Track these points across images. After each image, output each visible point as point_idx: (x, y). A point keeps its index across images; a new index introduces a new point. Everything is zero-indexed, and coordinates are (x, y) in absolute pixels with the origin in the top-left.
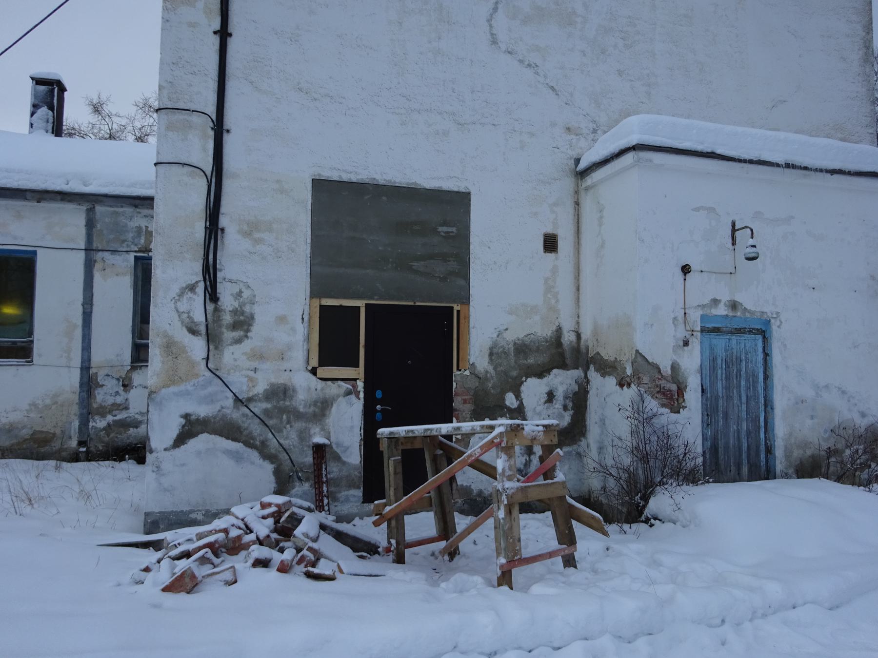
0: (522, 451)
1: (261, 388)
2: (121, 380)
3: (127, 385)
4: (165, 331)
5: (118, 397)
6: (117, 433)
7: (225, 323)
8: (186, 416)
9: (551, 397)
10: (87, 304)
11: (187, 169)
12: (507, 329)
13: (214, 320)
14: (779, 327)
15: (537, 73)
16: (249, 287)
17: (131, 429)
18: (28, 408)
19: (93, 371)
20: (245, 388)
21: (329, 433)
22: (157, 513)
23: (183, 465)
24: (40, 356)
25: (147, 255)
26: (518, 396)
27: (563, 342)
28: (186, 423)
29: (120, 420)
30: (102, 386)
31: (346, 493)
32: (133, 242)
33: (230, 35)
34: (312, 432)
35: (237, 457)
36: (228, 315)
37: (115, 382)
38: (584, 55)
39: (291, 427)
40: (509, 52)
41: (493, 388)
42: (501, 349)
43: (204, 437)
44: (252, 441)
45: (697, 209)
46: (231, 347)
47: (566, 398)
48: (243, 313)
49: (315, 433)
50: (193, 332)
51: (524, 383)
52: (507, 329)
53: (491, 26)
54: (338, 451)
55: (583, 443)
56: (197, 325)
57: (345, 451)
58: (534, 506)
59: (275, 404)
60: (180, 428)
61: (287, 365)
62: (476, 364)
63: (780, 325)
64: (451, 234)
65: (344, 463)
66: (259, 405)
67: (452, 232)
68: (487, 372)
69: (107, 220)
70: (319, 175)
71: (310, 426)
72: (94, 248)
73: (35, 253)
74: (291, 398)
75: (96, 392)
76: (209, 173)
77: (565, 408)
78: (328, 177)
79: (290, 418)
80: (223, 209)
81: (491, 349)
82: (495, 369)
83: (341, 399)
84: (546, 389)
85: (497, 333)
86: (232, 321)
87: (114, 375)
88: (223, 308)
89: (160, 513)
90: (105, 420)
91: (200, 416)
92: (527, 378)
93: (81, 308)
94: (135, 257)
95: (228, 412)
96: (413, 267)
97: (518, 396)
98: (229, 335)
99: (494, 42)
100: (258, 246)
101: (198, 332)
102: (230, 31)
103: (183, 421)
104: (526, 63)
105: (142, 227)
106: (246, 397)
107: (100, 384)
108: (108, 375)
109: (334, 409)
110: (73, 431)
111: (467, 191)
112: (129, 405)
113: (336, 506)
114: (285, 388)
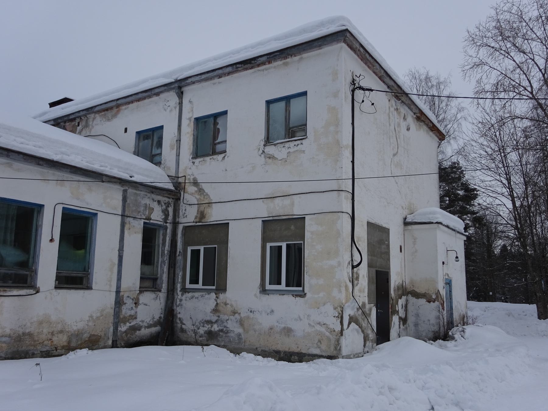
3: (136, 304)
6: (131, 335)
10: (121, 250)
11: (348, 215)
17: (137, 331)
18: (88, 319)
19: (121, 294)
24: (96, 283)
29: (133, 326)
30: (126, 303)
33: (351, 162)
35: (358, 332)
37: (131, 301)
50: (350, 281)
69: (132, 198)
70: (368, 220)
72: (126, 215)
73: (96, 214)
75: (123, 307)
83: (373, 308)
89: (346, 355)
90: (125, 326)
93: (118, 252)
94: (144, 222)
108: (128, 297)
110: (110, 334)
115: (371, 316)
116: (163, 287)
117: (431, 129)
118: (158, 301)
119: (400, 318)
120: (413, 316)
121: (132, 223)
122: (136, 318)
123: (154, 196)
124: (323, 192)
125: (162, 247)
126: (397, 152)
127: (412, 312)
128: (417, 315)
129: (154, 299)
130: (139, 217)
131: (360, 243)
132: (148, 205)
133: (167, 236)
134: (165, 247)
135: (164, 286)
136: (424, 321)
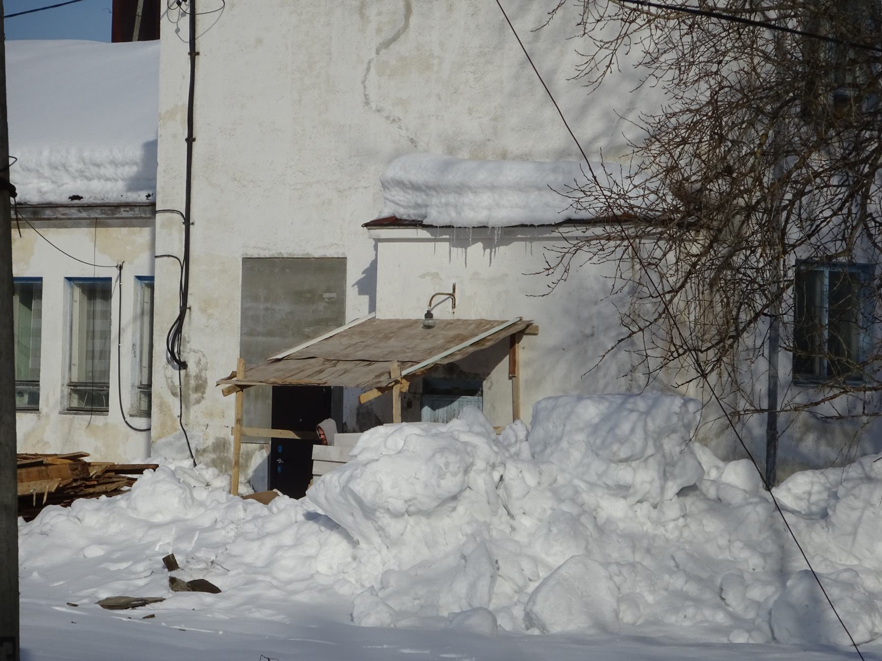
1: (210, 442)
14: (490, 388)
15: (400, 128)
20: (201, 440)
38: (440, 99)
40: (379, 111)
42: (365, 410)
45: (423, 276)
50: (174, 394)
53: (365, 87)
62: (347, 424)
63: (491, 386)
64: (332, 300)
67: (333, 298)
70: (246, 254)
78: (252, 255)
80: (190, 291)
81: (358, 409)
98: (194, 396)
99: (367, 103)
104: (391, 119)
106: (202, 448)
111: (344, 256)
131: (210, 311)
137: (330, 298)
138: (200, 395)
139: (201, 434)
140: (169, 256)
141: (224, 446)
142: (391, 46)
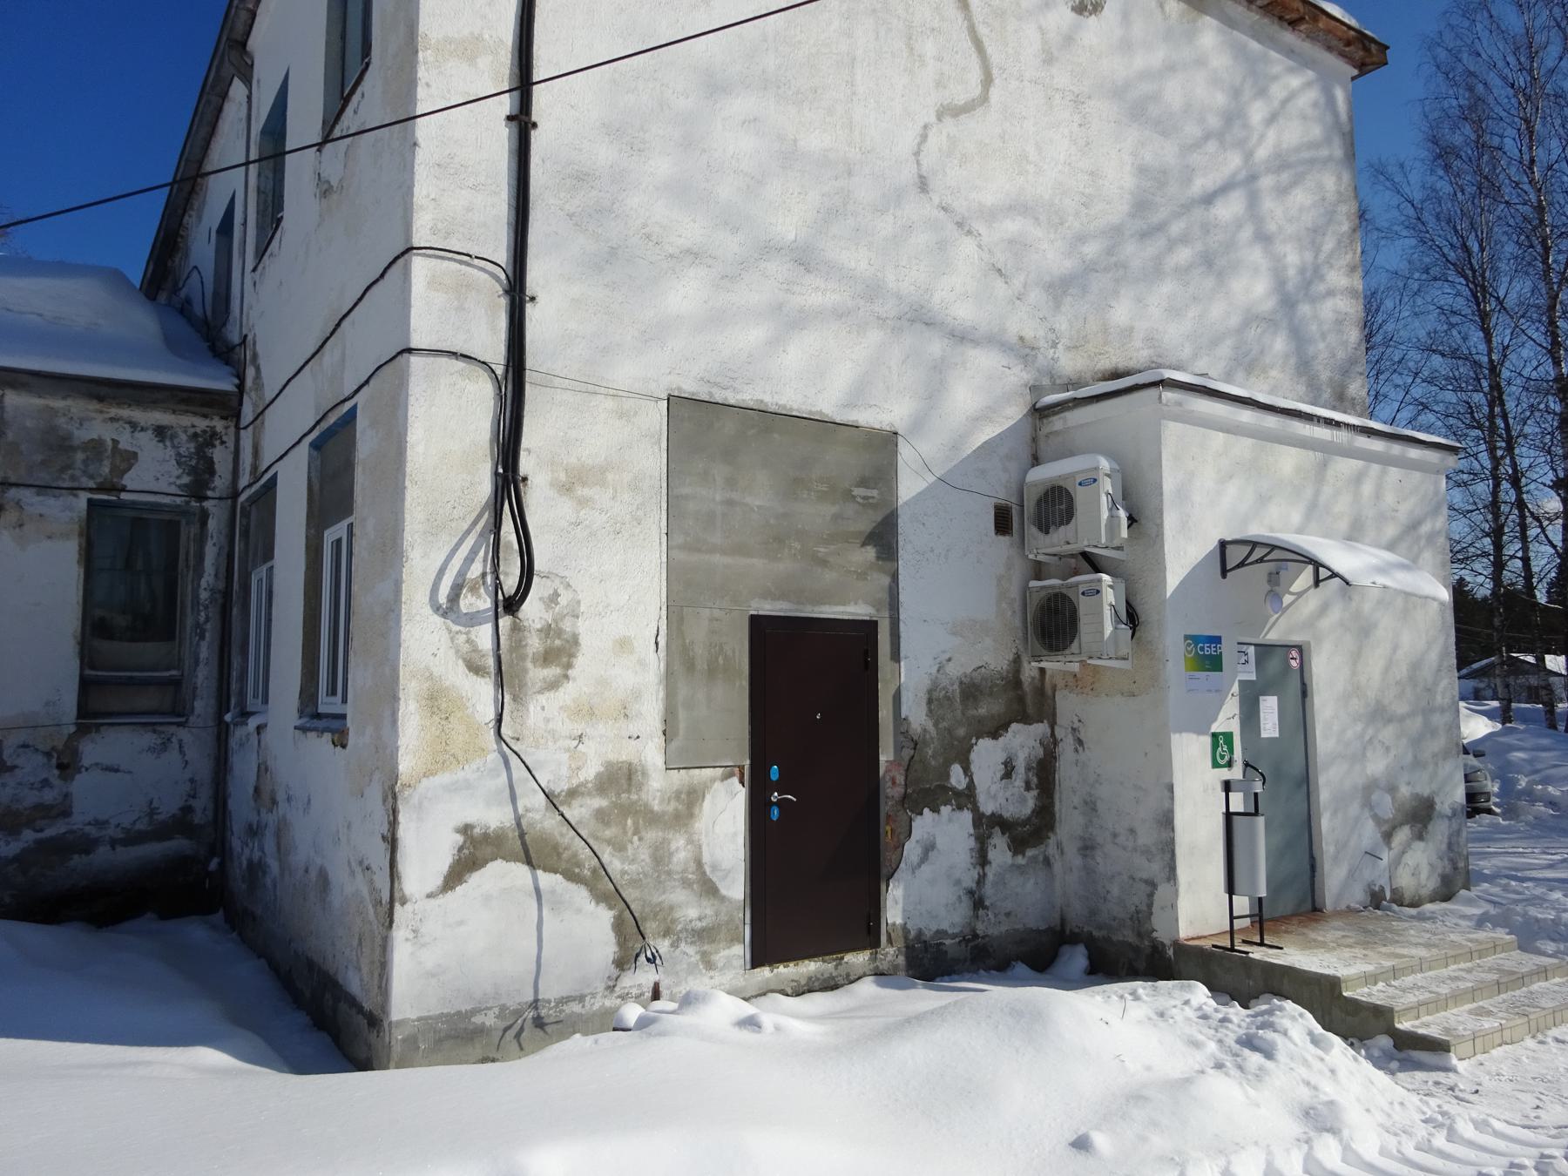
0: (973, 861)
1: (591, 772)
2: (55, 755)
3: (67, 765)
4: (427, 668)
5: (46, 790)
7: (530, 651)
8: (466, 830)
9: (1008, 771)
12: (949, 660)
13: (511, 646)
16: (569, 585)
17: (76, 857)
20: (564, 771)
21: (700, 847)
22: (413, 1021)
23: (461, 923)
25: (114, 498)
26: (967, 770)
27: (1023, 680)
28: (465, 842)
29: (52, 839)
30: (15, 767)
31: (726, 953)
32: (84, 472)
34: (673, 846)
36: (535, 637)
37: (41, 759)
39: (640, 839)
41: (933, 757)
43: (497, 867)
44: (577, 870)
46: (542, 699)
47: (1028, 769)
48: (559, 633)
49: (677, 849)
50: (475, 669)
51: (975, 747)
52: (949, 660)
54: (714, 879)
55: (1052, 841)
56: (483, 656)
57: (726, 876)
58: (991, 950)
59: (614, 799)
60: (456, 852)
61: (633, 728)
62: (911, 719)
64: (871, 501)
65: (723, 899)
66: (589, 802)
67: (873, 497)
68: (925, 730)
70: (679, 389)
71: (671, 836)
74: (640, 787)
76: (500, 371)
77: (1028, 787)
79: (638, 823)
81: (930, 692)
82: (936, 725)
84: (1002, 757)
85: (936, 668)
86: (541, 649)
87: (41, 747)
88: (526, 624)
89: (419, 1019)
91: (489, 827)
92: (977, 739)
94: (90, 501)
95: (538, 817)
96: (819, 555)
97: (967, 770)
98: (538, 674)
100: (583, 512)
101: (485, 668)
102: (534, 118)
103: (460, 839)
105: (105, 441)
106: (566, 788)
107: (9, 764)
109: (707, 804)
112: (71, 807)
113: (711, 978)
114: (630, 770)
115: (700, 825)
116: (197, 712)
117: (1281, 18)
118: (173, 755)
119: (986, 825)
120: (1075, 808)
121: (32, 505)
122: (66, 813)
123: (114, 411)
124: (382, 276)
125: (193, 581)
126: (984, 99)
127: (1074, 792)
128: (1091, 806)
129: (151, 750)
130: (65, 485)
132: (110, 443)
133: (210, 543)
134: (201, 577)
135: (203, 706)
136: (1115, 835)
137: (865, 498)
138: (552, 672)
139: (565, 757)
140: (453, 354)
141: (630, 778)
142: (963, 117)
